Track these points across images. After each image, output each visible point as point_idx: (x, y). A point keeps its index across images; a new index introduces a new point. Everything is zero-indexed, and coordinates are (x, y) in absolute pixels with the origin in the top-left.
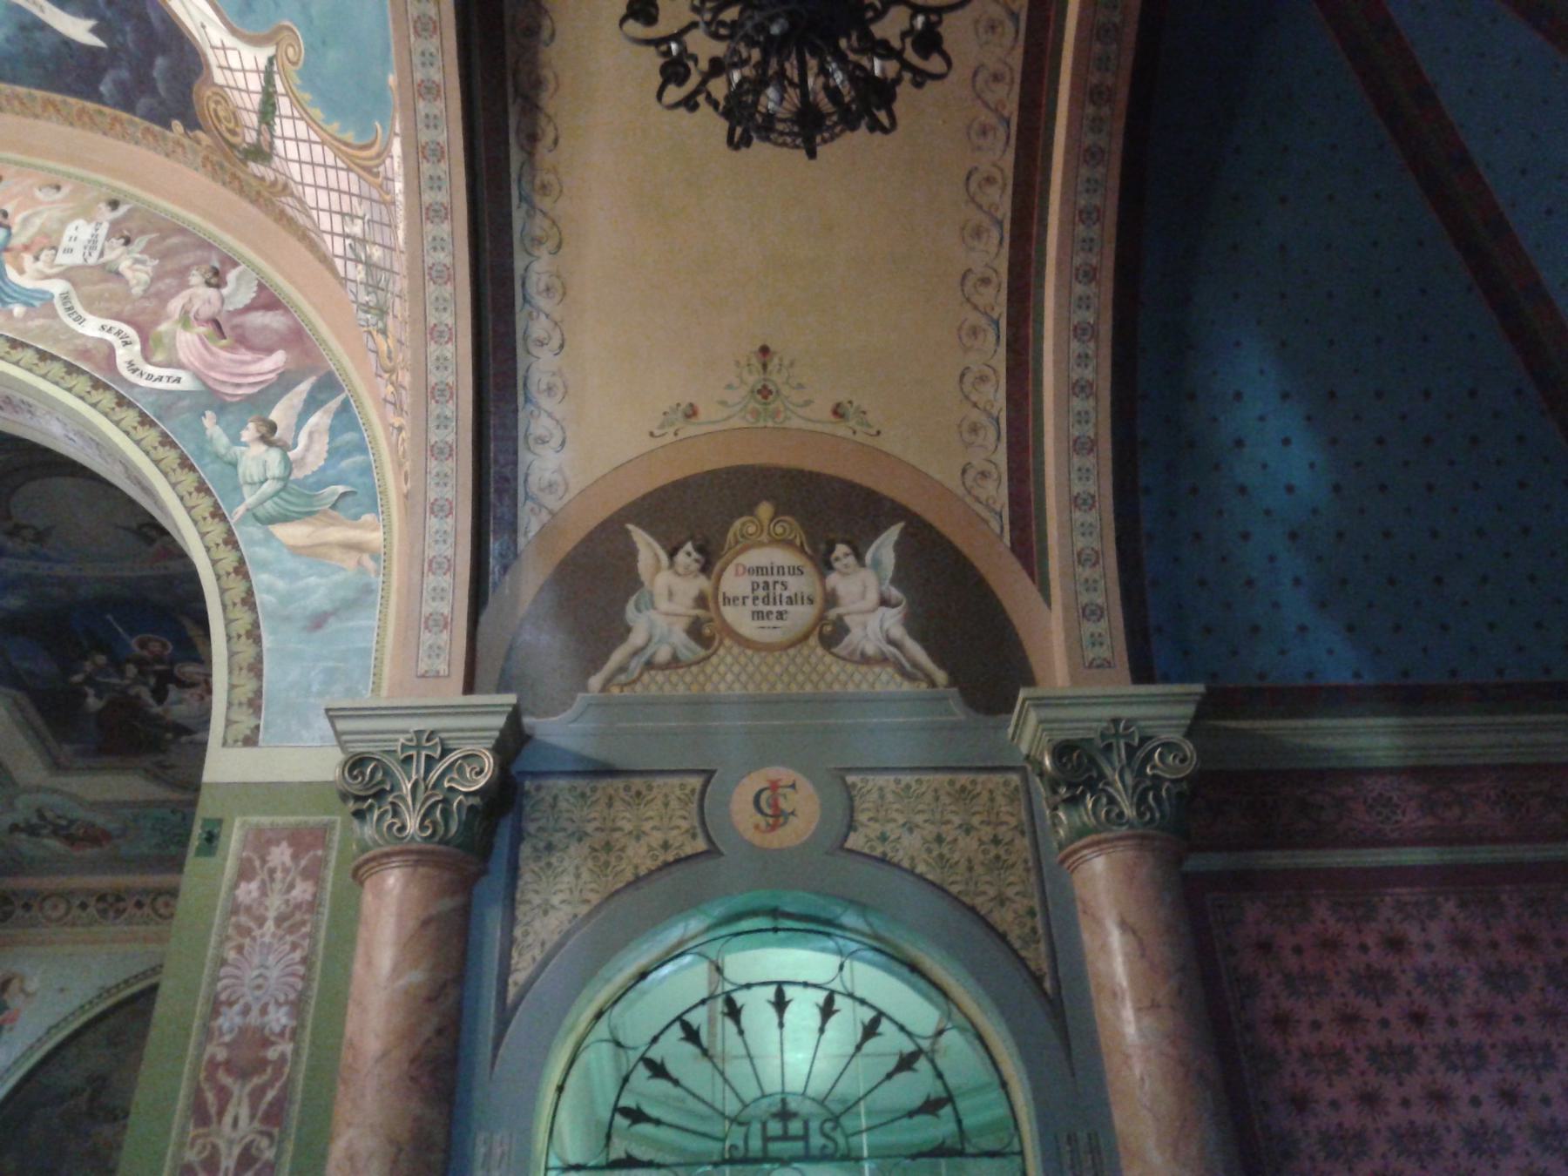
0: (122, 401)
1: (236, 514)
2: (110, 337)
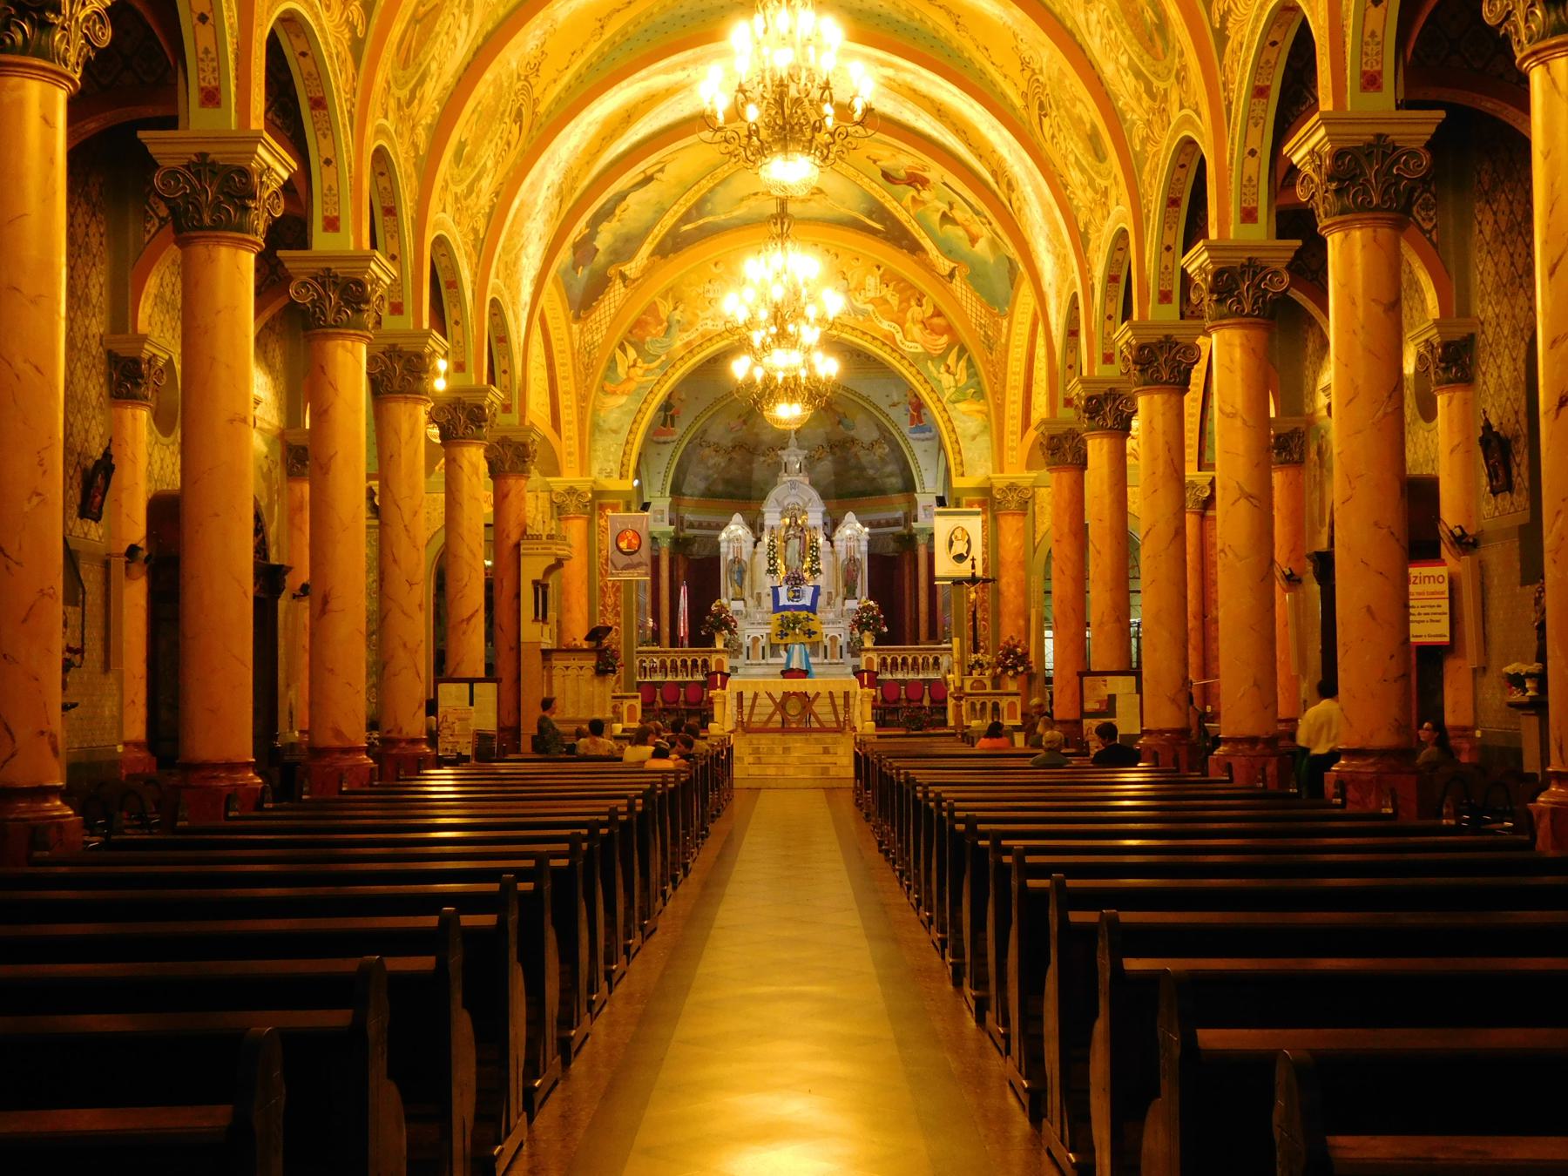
0: (903, 357)
1: (944, 400)
2: (892, 330)
